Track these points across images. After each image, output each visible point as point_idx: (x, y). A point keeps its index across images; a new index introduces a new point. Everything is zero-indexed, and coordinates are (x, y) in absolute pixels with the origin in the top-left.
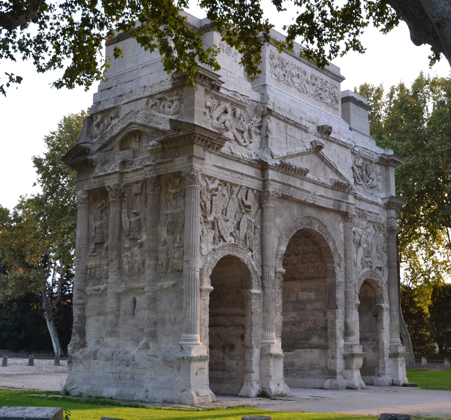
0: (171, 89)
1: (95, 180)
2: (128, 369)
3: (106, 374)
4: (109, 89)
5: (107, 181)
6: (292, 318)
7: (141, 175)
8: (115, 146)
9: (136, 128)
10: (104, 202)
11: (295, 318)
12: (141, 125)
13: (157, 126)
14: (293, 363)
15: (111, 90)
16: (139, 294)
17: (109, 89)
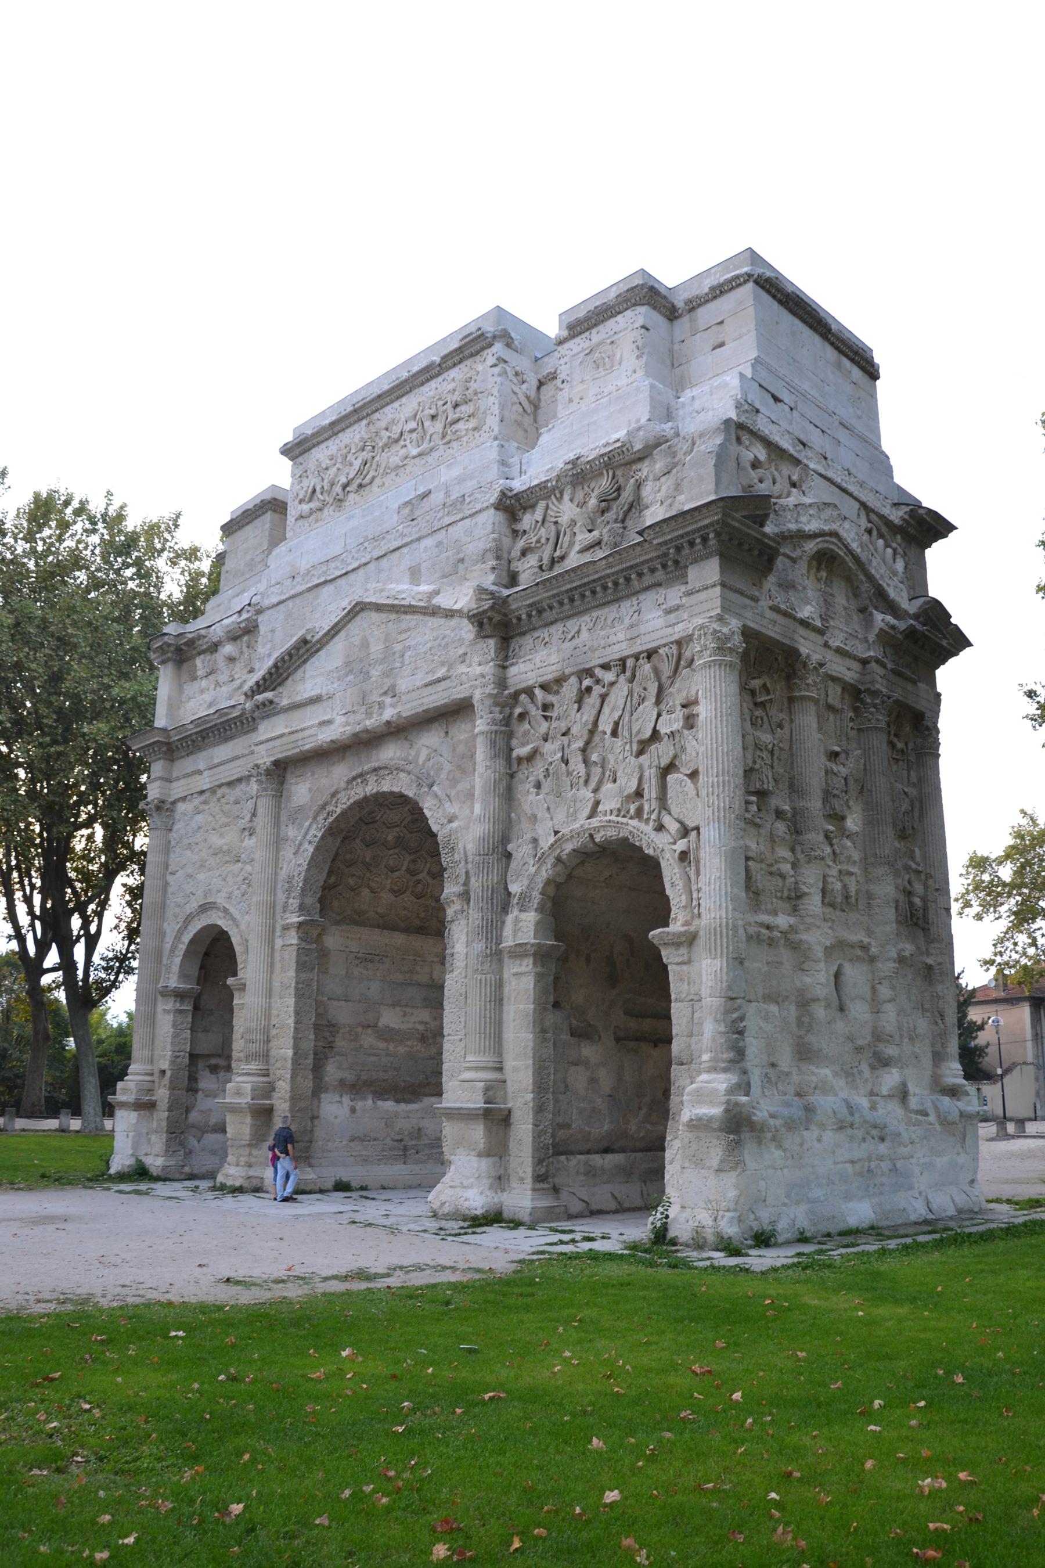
0: (895, 526)
1: (774, 616)
2: (883, 1148)
3: (840, 1165)
4: (777, 399)
5: (802, 641)
6: (421, 1023)
7: (849, 669)
8: (801, 558)
9: (841, 553)
10: (768, 685)
11: (426, 1023)
12: (853, 555)
13: (885, 585)
14: (419, 1129)
15: (779, 404)
16: (851, 960)
17: (777, 399)
